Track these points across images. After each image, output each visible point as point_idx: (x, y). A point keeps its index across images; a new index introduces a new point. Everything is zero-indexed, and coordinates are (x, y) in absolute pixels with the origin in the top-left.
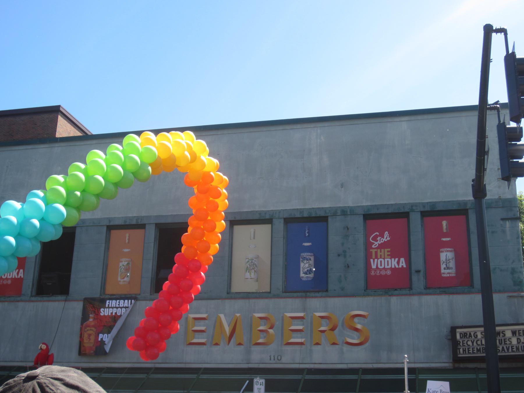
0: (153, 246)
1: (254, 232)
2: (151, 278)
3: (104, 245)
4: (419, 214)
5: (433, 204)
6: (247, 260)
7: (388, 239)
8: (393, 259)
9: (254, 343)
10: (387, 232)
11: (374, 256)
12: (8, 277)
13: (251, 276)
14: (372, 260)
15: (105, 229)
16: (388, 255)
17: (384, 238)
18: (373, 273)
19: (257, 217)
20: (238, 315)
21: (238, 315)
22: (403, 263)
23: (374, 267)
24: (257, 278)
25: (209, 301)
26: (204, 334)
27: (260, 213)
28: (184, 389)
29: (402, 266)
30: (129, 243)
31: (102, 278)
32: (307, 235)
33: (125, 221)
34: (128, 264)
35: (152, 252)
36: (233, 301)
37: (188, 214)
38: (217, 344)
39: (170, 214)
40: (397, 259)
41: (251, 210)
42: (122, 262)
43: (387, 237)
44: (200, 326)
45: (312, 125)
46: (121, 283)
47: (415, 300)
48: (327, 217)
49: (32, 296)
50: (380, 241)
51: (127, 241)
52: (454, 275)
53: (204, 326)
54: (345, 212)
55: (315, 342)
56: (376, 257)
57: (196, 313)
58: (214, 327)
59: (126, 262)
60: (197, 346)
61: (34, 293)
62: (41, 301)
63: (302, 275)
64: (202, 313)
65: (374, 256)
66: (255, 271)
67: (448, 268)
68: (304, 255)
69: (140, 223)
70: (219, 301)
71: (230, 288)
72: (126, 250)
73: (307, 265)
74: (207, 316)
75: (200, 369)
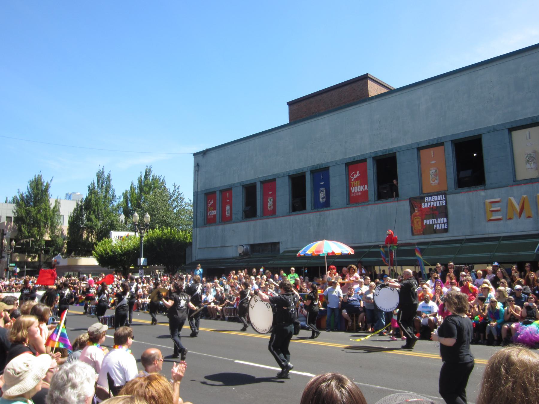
1: (529, 134)
3: (417, 161)
4: (507, 130)
5: (354, 158)
6: (526, 155)
7: (359, 175)
8: (361, 186)
9: (488, 220)
11: (352, 186)
12: (212, 214)
13: (531, 167)
14: (352, 188)
15: (416, 150)
16: (359, 184)
17: (356, 174)
18: (352, 195)
19: (435, 142)
20: (525, 196)
21: (525, 196)
22: (366, 188)
23: (353, 192)
24: (537, 168)
26: (500, 212)
27: (532, 118)
30: (434, 157)
31: (419, 183)
33: (429, 143)
34: (435, 171)
35: (452, 160)
36: (519, 187)
38: (510, 219)
39: (460, 132)
40: (363, 186)
41: (523, 118)
42: (431, 170)
43: (358, 174)
44: (496, 207)
45: (458, 75)
46: (269, 210)
47: (307, 216)
48: (329, 167)
49: (312, 210)
50: (356, 176)
52: (229, 216)
53: (499, 207)
54: (336, 164)
56: (354, 186)
57: (491, 198)
58: (507, 206)
59: (434, 169)
61: (291, 211)
63: (321, 200)
65: (352, 186)
66: (535, 163)
68: (321, 189)
69: (439, 142)
70: (508, 188)
72: (270, 193)
73: (322, 194)
74: (501, 200)
75: (462, 240)
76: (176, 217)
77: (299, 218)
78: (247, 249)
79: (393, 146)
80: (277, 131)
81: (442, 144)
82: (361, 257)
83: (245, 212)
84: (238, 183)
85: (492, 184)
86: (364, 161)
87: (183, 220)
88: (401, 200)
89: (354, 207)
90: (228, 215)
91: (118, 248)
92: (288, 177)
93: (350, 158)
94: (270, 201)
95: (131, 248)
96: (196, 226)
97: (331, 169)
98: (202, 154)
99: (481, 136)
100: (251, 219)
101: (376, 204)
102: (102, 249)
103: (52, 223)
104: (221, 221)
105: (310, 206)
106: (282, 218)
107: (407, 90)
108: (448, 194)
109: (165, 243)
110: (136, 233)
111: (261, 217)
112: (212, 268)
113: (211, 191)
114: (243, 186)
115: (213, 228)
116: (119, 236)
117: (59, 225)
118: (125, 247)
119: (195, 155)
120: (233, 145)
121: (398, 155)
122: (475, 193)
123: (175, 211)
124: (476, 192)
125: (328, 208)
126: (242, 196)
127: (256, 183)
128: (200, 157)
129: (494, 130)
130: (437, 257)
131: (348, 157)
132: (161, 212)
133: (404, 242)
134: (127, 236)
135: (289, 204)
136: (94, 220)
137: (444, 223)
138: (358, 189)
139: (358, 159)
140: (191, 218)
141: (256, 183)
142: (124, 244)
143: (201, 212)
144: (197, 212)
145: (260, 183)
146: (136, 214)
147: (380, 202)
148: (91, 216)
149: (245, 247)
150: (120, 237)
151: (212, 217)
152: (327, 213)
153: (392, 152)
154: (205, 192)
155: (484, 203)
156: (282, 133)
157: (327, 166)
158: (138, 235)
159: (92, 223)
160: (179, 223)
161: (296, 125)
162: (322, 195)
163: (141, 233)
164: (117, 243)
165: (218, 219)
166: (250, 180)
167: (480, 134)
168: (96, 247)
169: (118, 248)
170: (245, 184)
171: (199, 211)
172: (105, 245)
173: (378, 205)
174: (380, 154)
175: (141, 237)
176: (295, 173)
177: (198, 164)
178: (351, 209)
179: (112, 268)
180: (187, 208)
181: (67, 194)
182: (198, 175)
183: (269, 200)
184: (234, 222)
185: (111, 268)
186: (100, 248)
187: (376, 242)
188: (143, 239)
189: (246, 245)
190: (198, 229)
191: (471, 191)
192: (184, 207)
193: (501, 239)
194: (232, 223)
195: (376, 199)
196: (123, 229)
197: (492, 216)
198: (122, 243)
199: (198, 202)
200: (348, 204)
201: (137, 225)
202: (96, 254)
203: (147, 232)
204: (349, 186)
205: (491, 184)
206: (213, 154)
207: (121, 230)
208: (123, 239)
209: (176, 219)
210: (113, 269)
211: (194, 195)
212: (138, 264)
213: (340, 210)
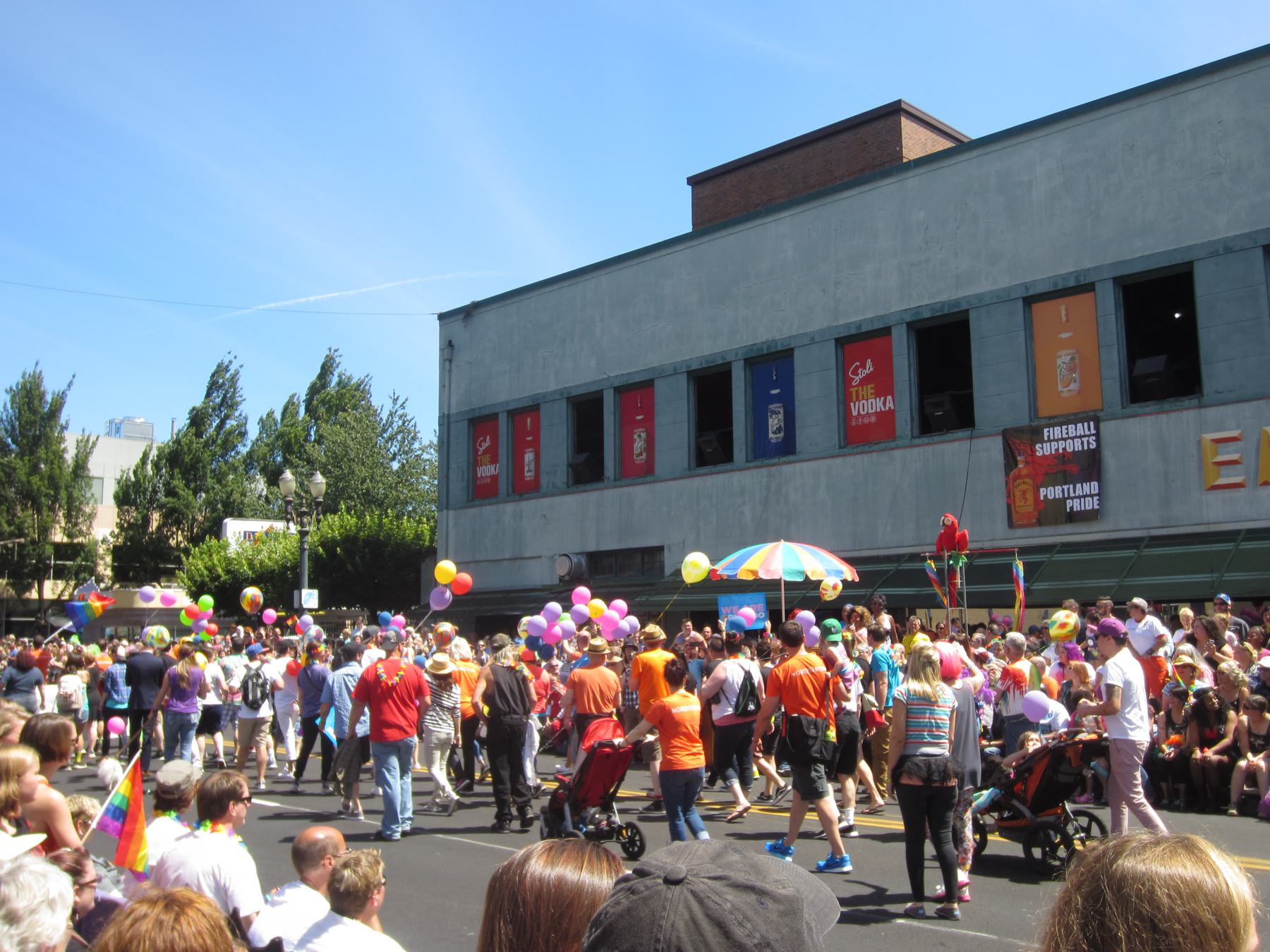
0: (835, 374)
2: (1118, 379)
3: (1022, 333)
4: (1261, 248)
5: (859, 325)
7: (871, 369)
8: (878, 399)
10: (869, 360)
11: (854, 398)
14: (852, 404)
15: (1020, 303)
16: (872, 394)
18: (854, 423)
19: (1072, 283)
22: (890, 405)
23: (855, 413)
25: (744, 472)
26: (1238, 466)
28: (1212, 572)
29: (890, 408)
30: (1067, 321)
31: (1029, 390)
32: (775, 378)
33: (1056, 284)
34: (1072, 359)
35: (1115, 331)
37: (1174, 250)
42: (1060, 357)
44: (1228, 453)
45: (1133, 103)
46: (637, 462)
47: (737, 478)
48: (792, 350)
49: (747, 461)
50: (863, 373)
51: (1064, 319)
52: (532, 478)
55: (1263, 480)
56: (858, 399)
57: (1216, 431)
58: (1258, 451)
59: (1068, 355)
60: (1226, 491)
61: (693, 463)
62: (931, 444)
63: (771, 435)
64: (1228, 430)
67: (529, 471)
68: (772, 407)
71: (1036, 410)
73: (776, 421)
75: (1140, 539)
76: (397, 483)
77: (714, 482)
78: (579, 563)
79: (961, 294)
80: (657, 254)
81: (1089, 288)
82: (878, 584)
83: (570, 465)
84: (555, 392)
85: (1221, 393)
86: (886, 332)
87: (417, 490)
88: (982, 436)
89: (856, 454)
90: (529, 475)
91: (244, 562)
92: (685, 375)
93: (848, 325)
94: (638, 440)
95: (277, 562)
96: (444, 502)
97: (797, 354)
98: (462, 316)
99: (1192, 266)
100: (588, 487)
101: (916, 446)
102: (201, 566)
103: (70, 498)
104: (510, 493)
105: (744, 453)
106: (671, 483)
107: (998, 146)
108: (1104, 420)
109: (367, 550)
110: (288, 523)
111: (615, 480)
112: (489, 614)
113: (486, 412)
114: (568, 399)
115: (489, 511)
116: (245, 533)
117: (88, 504)
118: (262, 562)
119: (442, 317)
120: (542, 291)
121: (973, 316)
122: (1174, 415)
123: (395, 466)
124: (1176, 413)
125: (791, 458)
126: (565, 424)
127: (601, 391)
128: (457, 325)
129: (1225, 249)
130: (1075, 584)
131: (842, 322)
132: (354, 466)
133: (987, 545)
134: (267, 533)
135: (689, 447)
136: (181, 492)
137: (1092, 496)
138: (868, 406)
139: (870, 328)
140: (436, 482)
141: (601, 391)
142: (260, 552)
143: (458, 467)
144: (448, 468)
145: (612, 390)
146: (288, 474)
147: (925, 440)
148: (176, 482)
149: (575, 560)
150: (248, 535)
151: (489, 481)
152: (787, 469)
153: (956, 310)
154: (470, 417)
155: (1199, 443)
156: (667, 258)
157: (788, 347)
158: (293, 528)
159: (175, 500)
160: (405, 498)
161: (705, 239)
162: (774, 422)
163: (302, 525)
164: (240, 550)
165: (503, 486)
166: (586, 384)
167: (1189, 260)
168: (188, 559)
169: (244, 562)
170: (574, 394)
171: (453, 465)
172: (211, 555)
173: (922, 449)
174: (927, 314)
175: (303, 534)
176: (704, 366)
177: (450, 342)
178: (851, 460)
179: (229, 616)
180: (425, 456)
181: (111, 422)
182: (450, 371)
183: (635, 436)
184: (545, 496)
185: (225, 616)
186: (196, 563)
187: (914, 546)
188: (308, 539)
189: (577, 554)
190: (451, 513)
191: (1163, 412)
192: (417, 456)
193: (1241, 537)
194: (540, 497)
195: (916, 432)
196: (257, 514)
197: (1219, 476)
198: (253, 551)
199: (453, 442)
200: (843, 445)
201: (288, 503)
202: (186, 580)
203: (319, 521)
204: (845, 399)
205: (1217, 392)
206: (489, 316)
207: (252, 516)
208: (256, 541)
209: (396, 486)
210: (231, 619)
211: (440, 425)
212: (296, 605)
213: (821, 461)
